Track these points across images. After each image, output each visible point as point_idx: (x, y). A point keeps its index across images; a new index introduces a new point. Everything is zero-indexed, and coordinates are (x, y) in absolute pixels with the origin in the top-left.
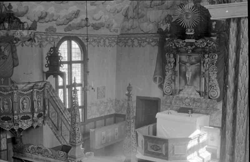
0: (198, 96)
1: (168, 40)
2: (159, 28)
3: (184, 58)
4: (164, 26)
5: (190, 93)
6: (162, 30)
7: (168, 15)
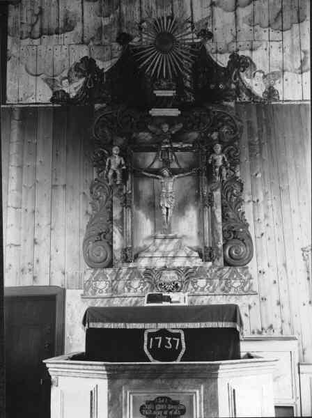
0: (198, 262)
1: (101, 110)
2: (56, 89)
3: (150, 160)
4: (75, 85)
5: (171, 255)
6: (68, 95)
7: (84, 59)
